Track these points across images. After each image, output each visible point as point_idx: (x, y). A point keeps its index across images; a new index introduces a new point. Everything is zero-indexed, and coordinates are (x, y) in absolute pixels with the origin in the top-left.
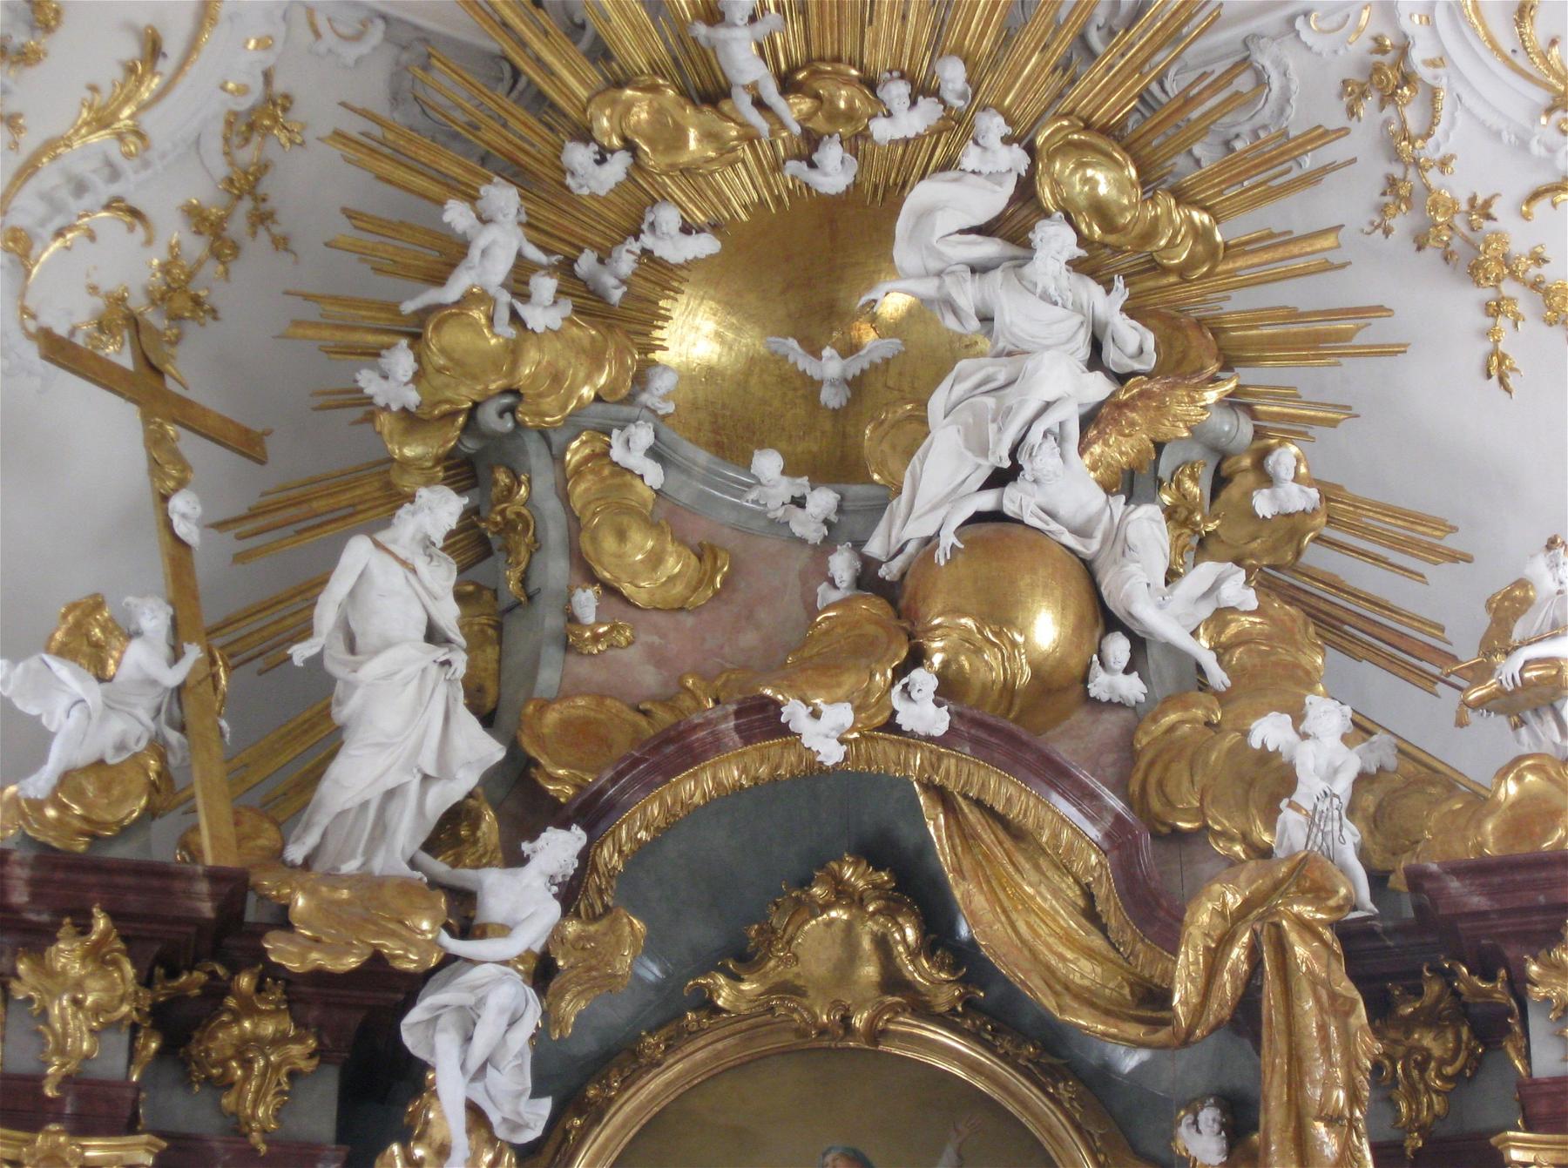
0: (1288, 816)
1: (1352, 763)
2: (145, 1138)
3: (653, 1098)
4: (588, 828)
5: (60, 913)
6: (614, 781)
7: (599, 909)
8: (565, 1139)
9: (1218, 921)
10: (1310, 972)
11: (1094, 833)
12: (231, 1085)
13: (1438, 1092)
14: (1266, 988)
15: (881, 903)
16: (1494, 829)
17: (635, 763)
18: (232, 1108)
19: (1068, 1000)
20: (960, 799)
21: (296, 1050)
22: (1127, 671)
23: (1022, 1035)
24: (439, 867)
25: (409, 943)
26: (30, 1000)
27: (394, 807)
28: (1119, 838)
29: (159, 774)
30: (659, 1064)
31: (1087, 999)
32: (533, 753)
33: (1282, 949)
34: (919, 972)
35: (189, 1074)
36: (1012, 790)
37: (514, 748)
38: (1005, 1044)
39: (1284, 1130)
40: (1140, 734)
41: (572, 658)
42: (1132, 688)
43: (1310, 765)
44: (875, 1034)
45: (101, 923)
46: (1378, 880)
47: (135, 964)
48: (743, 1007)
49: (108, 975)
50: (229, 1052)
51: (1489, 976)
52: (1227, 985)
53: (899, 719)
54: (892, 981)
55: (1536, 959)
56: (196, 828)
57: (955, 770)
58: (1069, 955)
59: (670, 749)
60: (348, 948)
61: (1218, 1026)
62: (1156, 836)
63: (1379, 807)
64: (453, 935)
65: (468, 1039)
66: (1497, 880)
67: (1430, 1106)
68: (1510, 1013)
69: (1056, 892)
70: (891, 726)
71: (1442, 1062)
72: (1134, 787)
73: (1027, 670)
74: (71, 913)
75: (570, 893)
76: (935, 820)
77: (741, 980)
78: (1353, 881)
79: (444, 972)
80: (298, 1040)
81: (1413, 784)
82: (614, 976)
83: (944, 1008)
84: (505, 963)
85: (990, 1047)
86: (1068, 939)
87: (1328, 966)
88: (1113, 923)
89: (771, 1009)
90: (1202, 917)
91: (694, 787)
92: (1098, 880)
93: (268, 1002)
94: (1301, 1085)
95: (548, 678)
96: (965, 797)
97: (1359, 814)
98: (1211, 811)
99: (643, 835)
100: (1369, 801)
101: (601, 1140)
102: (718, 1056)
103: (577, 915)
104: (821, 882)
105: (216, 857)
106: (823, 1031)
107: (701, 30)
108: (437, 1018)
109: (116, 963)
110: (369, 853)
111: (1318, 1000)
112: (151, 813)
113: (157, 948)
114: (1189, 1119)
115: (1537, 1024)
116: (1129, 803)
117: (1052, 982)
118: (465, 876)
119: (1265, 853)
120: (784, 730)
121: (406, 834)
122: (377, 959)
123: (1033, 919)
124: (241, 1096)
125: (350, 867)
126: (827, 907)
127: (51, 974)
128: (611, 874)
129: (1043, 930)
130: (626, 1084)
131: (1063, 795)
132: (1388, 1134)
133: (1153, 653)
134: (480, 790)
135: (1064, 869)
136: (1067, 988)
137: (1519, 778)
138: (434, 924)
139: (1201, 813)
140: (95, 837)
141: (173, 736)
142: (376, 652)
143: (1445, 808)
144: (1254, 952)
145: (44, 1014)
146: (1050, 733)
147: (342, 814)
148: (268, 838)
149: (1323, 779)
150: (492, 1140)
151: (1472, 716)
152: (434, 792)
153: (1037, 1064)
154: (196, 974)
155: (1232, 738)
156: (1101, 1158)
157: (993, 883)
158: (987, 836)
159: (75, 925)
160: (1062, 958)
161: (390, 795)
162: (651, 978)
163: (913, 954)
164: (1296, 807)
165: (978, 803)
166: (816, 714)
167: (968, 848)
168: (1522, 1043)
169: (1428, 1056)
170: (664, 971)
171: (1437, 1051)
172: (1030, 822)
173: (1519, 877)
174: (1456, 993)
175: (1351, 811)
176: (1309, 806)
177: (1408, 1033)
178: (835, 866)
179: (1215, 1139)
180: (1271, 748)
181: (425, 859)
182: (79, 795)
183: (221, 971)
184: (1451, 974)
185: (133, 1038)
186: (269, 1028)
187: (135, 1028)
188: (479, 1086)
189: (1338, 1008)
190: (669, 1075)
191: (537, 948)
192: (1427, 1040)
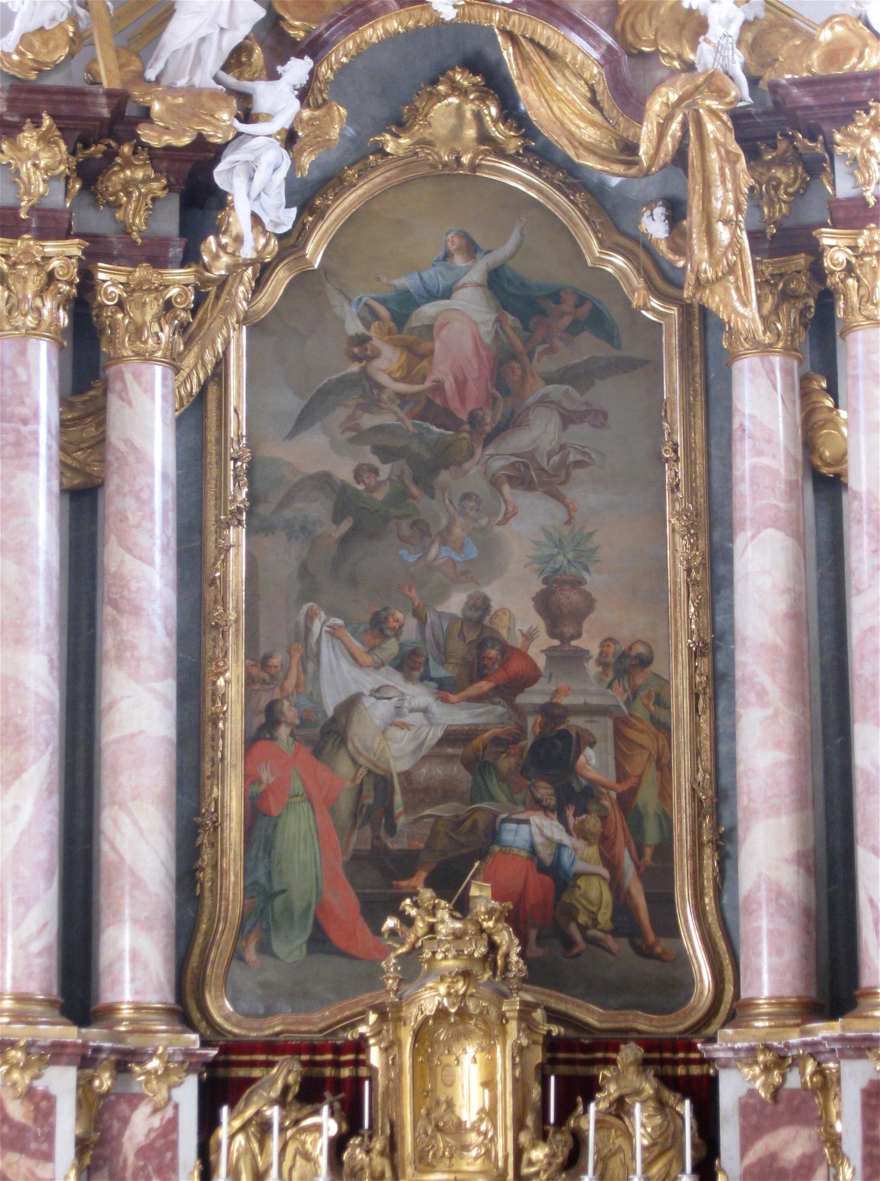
0: (703, 46)
2: (77, 241)
3: (351, 206)
4: (312, 57)
5: (24, 116)
6: (327, 29)
7: (320, 101)
8: (304, 228)
9: (664, 108)
10: (715, 139)
11: (596, 55)
12: (120, 206)
13: (785, 202)
14: (691, 146)
15: (477, 94)
16: (818, 57)
17: (339, 19)
18: (122, 218)
19: (581, 151)
20: (521, 38)
21: (155, 185)
23: (558, 167)
24: (230, 79)
25: (216, 127)
26: (9, 164)
27: (205, 48)
28: (610, 60)
29: (74, 33)
30: (354, 186)
31: (591, 149)
32: (281, 12)
34: (498, 131)
35: (97, 200)
36: (550, 33)
37: (269, 8)
38: (546, 172)
39: (700, 225)
44: (474, 167)
45: (47, 121)
46: (753, 82)
47: (66, 143)
48: (401, 152)
49: (51, 149)
51: (813, 139)
52: (669, 144)
54: (484, 137)
55: (839, 131)
56: (95, 60)
58: (582, 125)
59: (358, 11)
60: (184, 133)
61: (665, 166)
62: (630, 55)
63: (755, 39)
64: (241, 121)
65: (251, 179)
66: (818, 88)
67: (781, 209)
69: (575, 90)
71: (788, 186)
72: (618, 27)
74: (30, 116)
75: (304, 94)
76: (507, 50)
77: (400, 137)
78: (739, 86)
79: (236, 141)
80: (156, 180)
81: (774, 26)
82: (329, 140)
83: (512, 152)
84: (269, 136)
85: (538, 174)
86: (582, 116)
87: (725, 136)
88: (606, 106)
89: (416, 154)
90: (656, 106)
91: (373, 33)
92: (598, 83)
93: (141, 160)
94: (710, 201)
96: (524, 37)
97: (743, 44)
98: (661, 42)
99: (344, 60)
100: (749, 37)
101: (324, 228)
102: (388, 179)
103: (308, 106)
104: (443, 83)
105: (109, 82)
106: (445, 165)
108: (234, 167)
109: (56, 143)
110: (192, 73)
111: (719, 153)
112: (71, 55)
113: (78, 133)
114: (648, 213)
117: (573, 141)
118: (246, 85)
119: (690, 67)
121: (213, 61)
122: (200, 136)
123: (562, 105)
124: (126, 213)
125: (182, 83)
126: (446, 96)
127: (20, 149)
128: (327, 82)
129: (567, 111)
130: (337, 197)
131: (578, 34)
132: (757, 225)
134: (252, 35)
135: (579, 76)
136: (581, 144)
137: (832, 28)
138: (230, 116)
139: (655, 43)
140: (40, 71)
141: (81, 12)
143: (791, 43)
145: (17, 172)
147: (175, 52)
148: (135, 66)
149: (723, 26)
150: (265, 232)
152: (227, 36)
153: (563, 183)
154: (100, 146)
156: (600, 235)
157: (540, 85)
158: (536, 59)
159: (33, 122)
160: (578, 127)
161: (203, 40)
162: (349, 135)
163: (495, 122)
164: (707, 41)
165: (531, 41)
167: (526, 66)
168: (831, 178)
169: (779, 182)
170: (356, 131)
171: (784, 179)
172: (560, 51)
173: (830, 87)
174: (795, 148)
175: (739, 42)
176: (715, 41)
177: (769, 169)
178: (451, 73)
179: (663, 224)
180: (694, 7)
181: (223, 75)
182: (30, 47)
183: (113, 144)
184: (792, 139)
185: (67, 183)
186: (140, 174)
187: (67, 178)
188: (257, 203)
189: (730, 159)
190: (360, 192)
191: (287, 127)
192: (779, 173)
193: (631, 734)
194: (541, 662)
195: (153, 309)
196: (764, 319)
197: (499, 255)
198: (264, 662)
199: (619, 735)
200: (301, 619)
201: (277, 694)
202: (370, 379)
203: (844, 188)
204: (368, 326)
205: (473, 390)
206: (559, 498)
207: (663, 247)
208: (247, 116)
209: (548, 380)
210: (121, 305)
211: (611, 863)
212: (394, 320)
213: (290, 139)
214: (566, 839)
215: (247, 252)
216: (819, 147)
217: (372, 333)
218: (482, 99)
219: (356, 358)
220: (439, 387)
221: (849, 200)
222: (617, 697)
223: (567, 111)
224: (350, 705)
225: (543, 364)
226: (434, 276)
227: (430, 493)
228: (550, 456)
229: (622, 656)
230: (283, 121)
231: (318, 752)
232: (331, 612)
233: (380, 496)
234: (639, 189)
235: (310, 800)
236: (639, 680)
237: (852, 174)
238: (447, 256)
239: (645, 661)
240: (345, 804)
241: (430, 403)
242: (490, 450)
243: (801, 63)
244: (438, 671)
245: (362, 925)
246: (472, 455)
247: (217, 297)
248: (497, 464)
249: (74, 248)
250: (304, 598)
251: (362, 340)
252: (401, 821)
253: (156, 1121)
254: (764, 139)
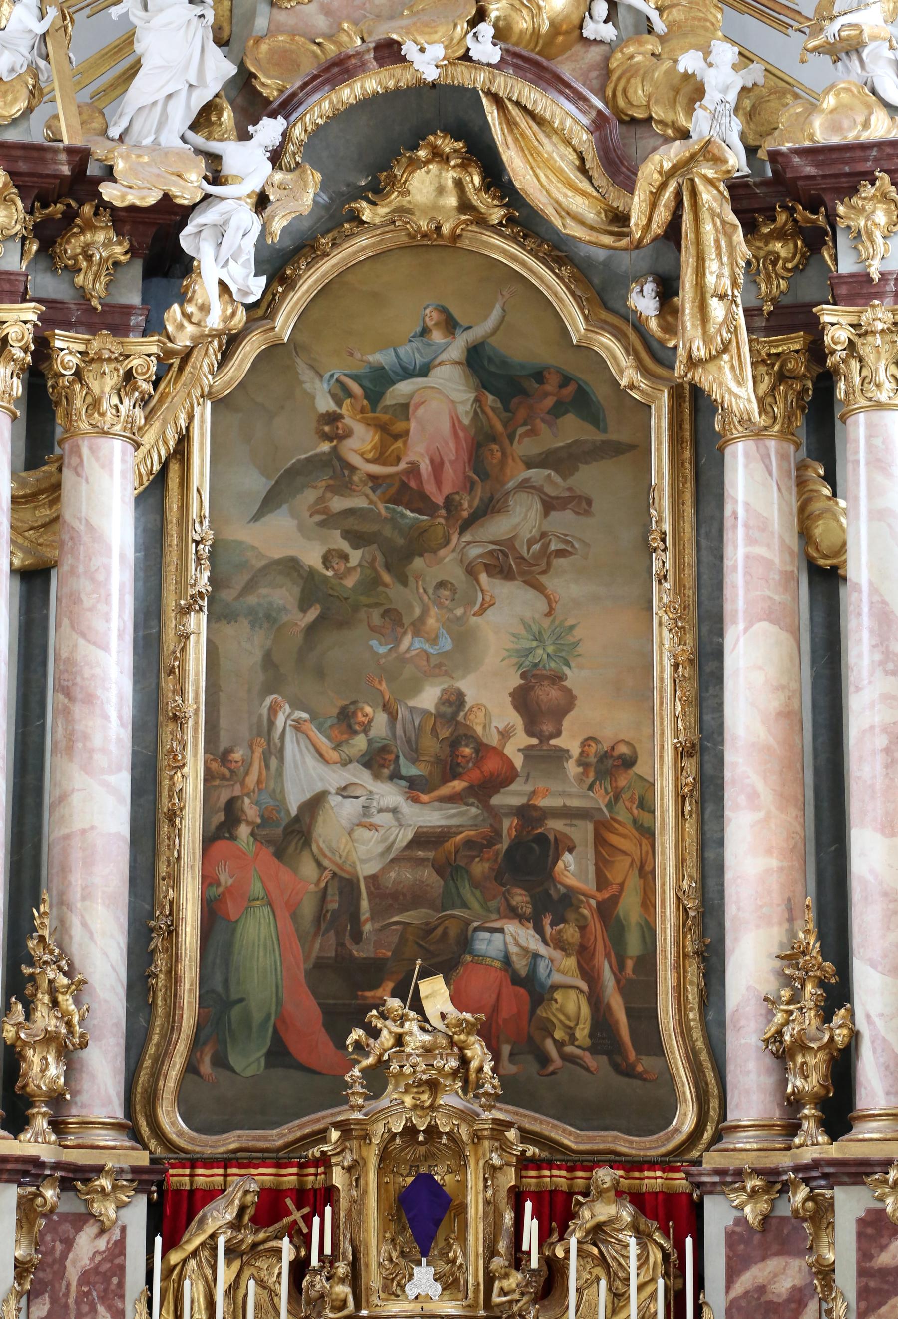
0: (699, 113)
1: (737, 81)
2: (33, 304)
3: (324, 276)
8: (274, 299)
10: (710, 209)
11: (585, 121)
13: (783, 278)
14: (685, 217)
15: (459, 161)
16: (821, 125)
18: (81, 283)
19: (568, 221)
22: (605, 22)
24: (198, 139)
27: (172, 103)
28: (599, 123)
29: (34, 87)
30: (328, 255)
32: (253, 70)
33: (694, 194)
35: (55, 264)
37: (242, 67)
40: (612, 60)
41: (275, 11)
42: (608, 32)
43: (714, 83)
44: (455, 237)
46: (751, 151)
47: (23, 200)
48: (377, 221)
50: (79, 251)
51: (815, 212)
53: (471, 54)
56: (56, 117)
57: (505, 84)
58: (570, 194)
61: (656, 239)
62: (621, 122)
63: (754, 107)
64: (209, 183)
66: (821, 157)
67: (778, 286)
68: (827, 236)
70: (466, 57)
71: (786, 260)
72: (609, 92)
73: (547, 23)
75: (276, 157)
76: (492, 113)
79: (204, 204)
87: (721, 206)
95: (261, 23)
96: (510, 99)
97: (741, 112)
100: (747, 103)
104: (425, 147)
105: (70, 138)
106: (425, 236)
108: (200, 231)
110: (158, 131)
111: (715, 225)
112: (30, 110)
113: (36, 192)
114: (638, 289)
115: (841, 240)
116: (606, 103)
117: (560, 210)
118: (215, 146)
119: (685, 135)
120: (403, 59)
122: (167, 197)
123: (549, 172)
130: (309, 266)
132: (754, 303)
133: (621, 11)
134: (222, 93)
135: (568, 142)
136: (568, 214)
141: (42, 63)
142: (161, 10)
144: (678, 195)
146: (559, 59)
151: (809, 56)
152: (196, 94)
154: (58, 206)
155: (667, 64)
156: (586, 312)
160: (566, 196)
162: (322, 201)
164: (705, 108)
165: (517, 104)
166: (422, 50)
167: (511, 131)
168: (832, 252)
169: (778, 257)
170: (330, 199)
171: (783, 253)
172: (548, 116)
173: (834, 156)
174: (795, 221)
175: (736, 110)
178: (431, 138)
179: (653, 301)
180: (690, 72)
181: (190, 135)
183: (74, 204)
185: (23, 245)
187: (24, 239)
188: (225, 270)
189: (726, 229)
190: (334, 261)
191: (258, 190)
193: (614, 839)
194: (518, 761)
195: (111, 381)
196: (761, 401)
198: (225, 758)
199: (600, 841)
200: (265, 711)
201: (237, 791)
202: (341, 459)
203: (846, 265)
204: (339, 404)
205: (449, 472)
206: (539, 588)
207: (653, 324)
208: (216, 177)
209: (529, 465)
210: (78, 374)
211: (589, 974)
212: (367, 397)
213: (262, 202)
214: (542, 950)
215: (214, 321)
216: (821, 219)
217: (344, 411)
218: (463, 166)
220: (414, 470)
221: (851, 275)
222: (599, 799)
223: (554, 179)
225: (524, 447)
226: (411, 353)
227: (403, 581)
228: (530, 543)
229: (605, 756)
230: (253, 185)
231: (280, 854)
232: (297, 704)
233: (350, 582)
234: (627, 262)
235: (270, 904)
236: (622, 782)
237: (855, 248)
238: (425, 331)
239: (628, 762)
240: (308, 909)
241: (404, 486)
242: (467, 537)
243: (802, 130)
245: (323, 1037)
246: (448, 541)
247: (181, 369)
248: (474, 551)
249: (30, 312)
250: (268, 689)
251: (333, 418)
252: (367, 927)
253: (102, 1244)
254: (760, 211)
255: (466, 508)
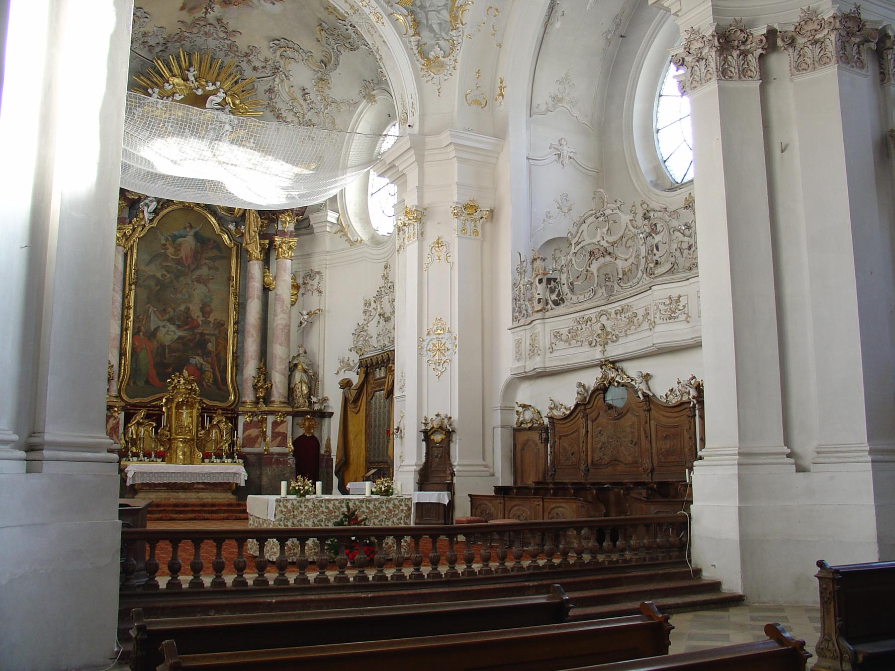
107: (187, 72)
194: (200, 323)
197: (197, 229)
206: (207, 286)
209: (206, 260)
211: (213, 368)
212: (172, 241)
214: (204, 363)
219: (163, 249)
220: (181, 258)
222: (217, 332)
224: (157, 329)
226: (182, 232)
229: (219, 323)
238: (185, 228)
244: (177, 323)
248: (194, 277)
252: (167, 356)
255: (193, 267)
